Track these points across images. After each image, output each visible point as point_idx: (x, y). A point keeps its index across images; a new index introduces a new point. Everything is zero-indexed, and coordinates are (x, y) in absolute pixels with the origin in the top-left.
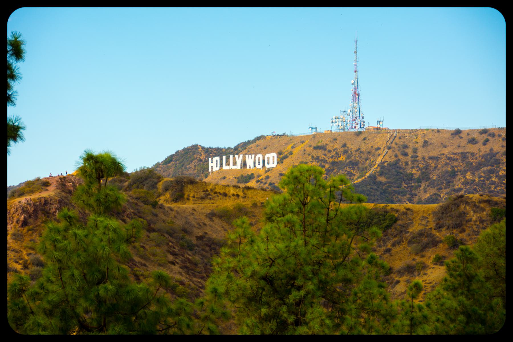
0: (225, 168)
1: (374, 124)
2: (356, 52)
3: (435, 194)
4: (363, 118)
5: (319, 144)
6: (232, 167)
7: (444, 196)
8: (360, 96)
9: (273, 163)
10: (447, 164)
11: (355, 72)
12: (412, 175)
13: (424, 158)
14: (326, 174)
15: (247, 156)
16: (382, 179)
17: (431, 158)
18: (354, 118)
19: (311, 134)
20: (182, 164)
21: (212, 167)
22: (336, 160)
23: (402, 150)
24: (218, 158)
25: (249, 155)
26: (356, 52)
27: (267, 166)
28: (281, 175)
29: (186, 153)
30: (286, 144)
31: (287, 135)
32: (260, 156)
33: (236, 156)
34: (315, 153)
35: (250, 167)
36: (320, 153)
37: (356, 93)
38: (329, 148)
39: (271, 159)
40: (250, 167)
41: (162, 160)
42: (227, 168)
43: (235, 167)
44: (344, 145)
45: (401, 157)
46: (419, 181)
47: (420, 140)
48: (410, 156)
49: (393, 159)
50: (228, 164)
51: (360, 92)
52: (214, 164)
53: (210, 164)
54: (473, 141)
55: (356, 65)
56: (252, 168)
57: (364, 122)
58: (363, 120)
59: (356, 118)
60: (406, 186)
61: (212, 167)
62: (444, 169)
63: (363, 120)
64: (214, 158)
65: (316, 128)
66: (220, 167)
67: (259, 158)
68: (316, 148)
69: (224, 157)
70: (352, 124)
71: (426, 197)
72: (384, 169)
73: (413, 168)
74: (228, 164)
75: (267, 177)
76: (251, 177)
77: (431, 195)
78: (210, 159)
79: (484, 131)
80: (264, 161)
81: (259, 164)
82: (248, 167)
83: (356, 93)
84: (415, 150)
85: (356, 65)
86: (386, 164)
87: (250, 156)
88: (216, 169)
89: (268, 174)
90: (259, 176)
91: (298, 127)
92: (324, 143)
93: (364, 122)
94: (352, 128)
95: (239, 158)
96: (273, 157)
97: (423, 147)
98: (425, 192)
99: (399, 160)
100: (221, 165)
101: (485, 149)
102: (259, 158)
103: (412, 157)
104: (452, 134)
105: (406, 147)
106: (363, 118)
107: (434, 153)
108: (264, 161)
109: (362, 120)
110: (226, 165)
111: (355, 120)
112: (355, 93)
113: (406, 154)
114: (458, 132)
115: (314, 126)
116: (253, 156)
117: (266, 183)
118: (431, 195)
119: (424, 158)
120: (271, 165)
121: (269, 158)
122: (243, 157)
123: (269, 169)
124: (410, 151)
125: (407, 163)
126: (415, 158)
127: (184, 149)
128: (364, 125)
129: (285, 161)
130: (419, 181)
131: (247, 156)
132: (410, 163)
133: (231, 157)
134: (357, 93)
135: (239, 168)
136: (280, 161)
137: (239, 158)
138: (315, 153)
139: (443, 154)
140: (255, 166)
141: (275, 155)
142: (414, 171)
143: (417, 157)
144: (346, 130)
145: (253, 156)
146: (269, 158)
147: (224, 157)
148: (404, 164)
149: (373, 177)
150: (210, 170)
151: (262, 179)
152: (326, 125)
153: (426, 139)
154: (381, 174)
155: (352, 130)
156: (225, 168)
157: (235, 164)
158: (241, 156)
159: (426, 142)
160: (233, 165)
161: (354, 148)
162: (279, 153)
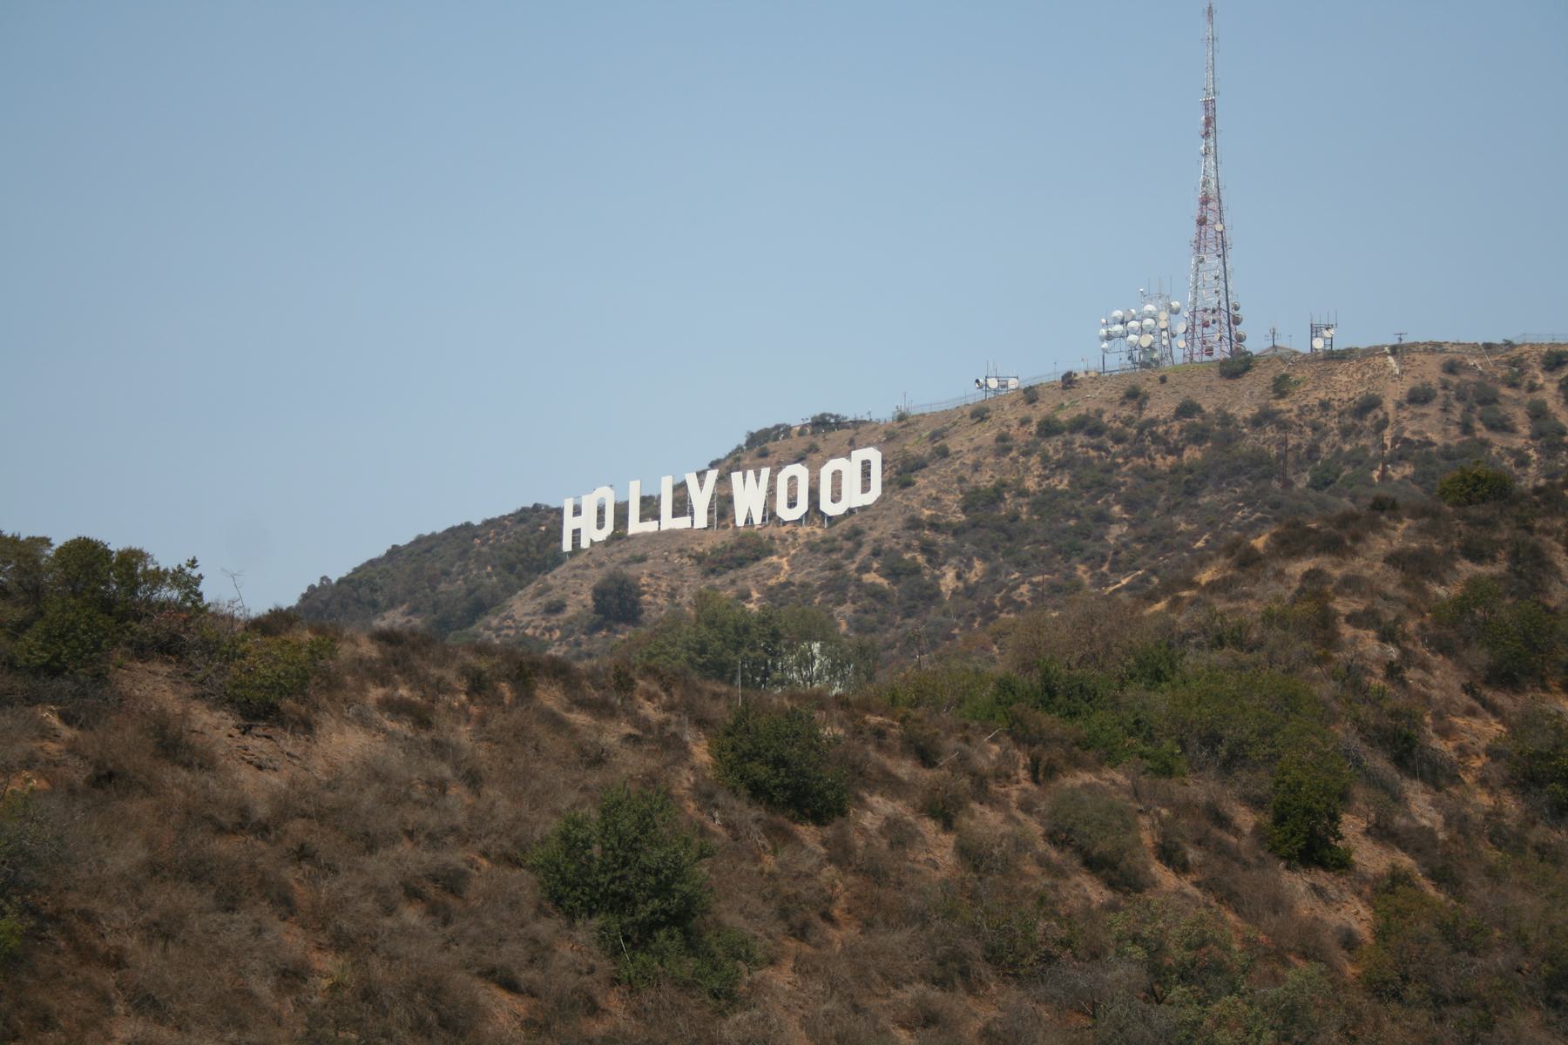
4: (1237, 321)
6: (668, 522)
9: (866, 488)
15: (736, 477)
21: (577, 532)
32: (800, 471)
35: (749, 520)
40: (749, 520)
42: (651, 526)
43: (683, 523)
55: (1209, 106)
56: (757, 520)
61: (577, 532)
71: (938, 994)
80: (814, 494)
81: (792, 504)
82: (740, 522)
85: (1209, 106)
95: (701, 483)
96: (866, 467)
108: (814, 494)
110: (642, 519)
116: (765, 472)
120: (854, 497)
121: (837, 476)
127: (420, 540)
131: (736, 477)
135: (701, 520)
137: (701, 483)
140: (773, 515)
150: (567, 546)
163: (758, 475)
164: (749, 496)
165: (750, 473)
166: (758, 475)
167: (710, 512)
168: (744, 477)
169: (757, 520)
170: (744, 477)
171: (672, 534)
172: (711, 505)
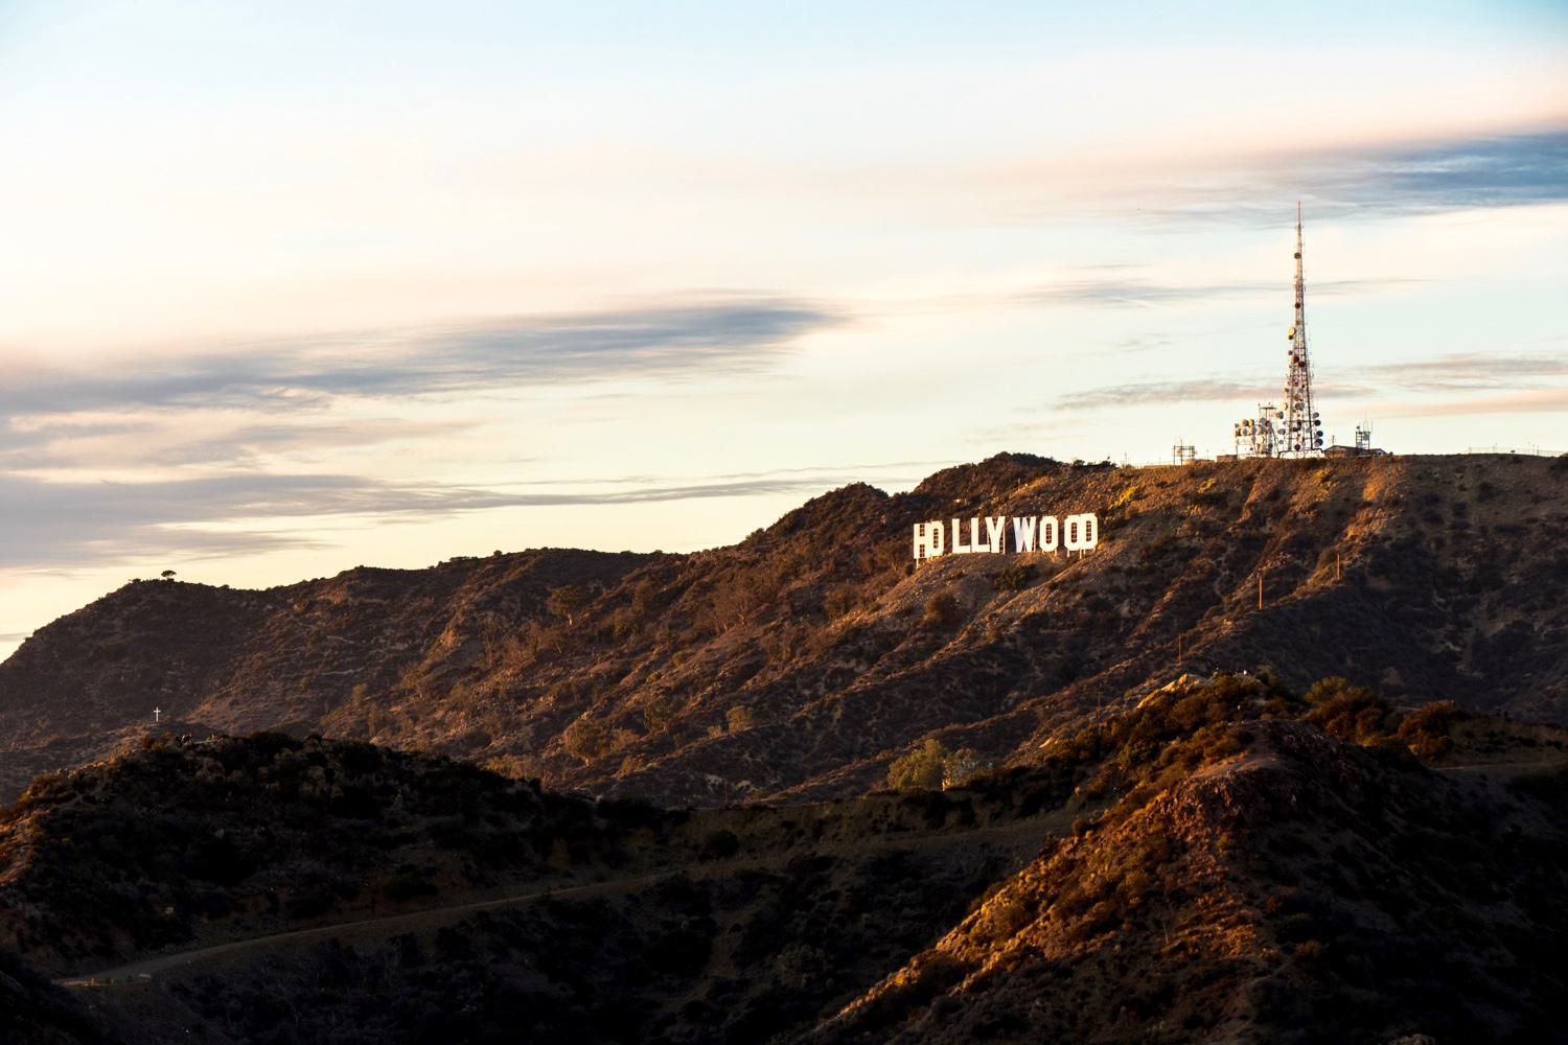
0: (958, 549)
2: (1298, 256)
3: (1517, 623)
4: (1318, 423)
6: (976, 547)
7: (1542, 629)
8: (1311, 369)
10: (1544, 546)
11: (1298, 306)
12: (1454, 571)
13: (1484, 530)
14: (1231, 569)
15: (1016, 521)
16: (1380, 584)
17: (1501, 530)
18: (1295, 425)
19: (1178, 463)
20: (828, 535)
21: (922, 546)
22: (1253, 531)
23: (1426, 508)
24: (939, 525)
25: (1021, 516)
26: (1298, 256)
27: (1070, 546)
29: (837, 506)
30: (1118, 488)
31: (1114, 465)
32: (1050, 520)
33: (989, 520)
37: (1300, 363)
39: (1082, 532)
41: (770, 524)
42: (965, 550)
43: (985, 549)
44: (1274, 495)
45: (1423, 527)
46: (1475, 587)
47: (1470, 481)
48: (1448, 524)
49: (1405, 533)
50: (966, 540)
51: (1311, 358)
52: (928, 540)
53: (917, 540)
56: (1029, 549)
57: (1320, 434)
58: (1319, 428)
59: (1299, 423)
60: (1442, 600)
61: (922, 546)
62: (1537, 558)
63: (1319, 428)
64: (927, 525)
65: (1192, 448)
66: (945, 545)
67: (1049, 527)
69: (956, 523)
70: (1290, 439)
73: (1456, 554)
74: (966, 540)
77: (1508, 626)
78: (917, 527)
80: (1061, 533)
82: (1019, 550)
84: (1460, 510)
86: (1387, 544)
87: (1024, 519)
88: (934, 552)
90: (1053, 571)
93: (1320, 434)
94: (1290, 449)
95: (995, 525)
96: (1089, 524)
97: (1481, 499)
98: (1493, 617)
99: (1420, 533)
102: (1049, 527)
103: (1453, 527)
104: (1552, 468)
105: (1434, 500)
106: (1318, 423)
107: (1509, 516)
108: (1061, 533)
109: (1315, 429)
111: (1296, 430)
112: (1296, 359)
113: (1436, 520)
115: (1186, 444)
116: (1033, 519)
117: (1075, 592)
118: (1508, 626)
119: (1484, 530)
122: (1006, 520)
123: (1076, 553)
124: (1449, 517)
125: (1440, 543)
126: (1460, 528)
128: (1321, 442)
130: (1475, 587)
131: (1016, 521)
132: (1448, 542)
133: (975, 522)
134: (1302, 359)
135: (996, 549)
136: (1107, 531)
137: (995, 525)
139: (1534, 520)
140: (1038, 547)
141: (1092, 518)
142: (1461, 563)
143: (1468, 526)
144: (1274, 456)
145: (1033, 519)
146: (1074, 527)
147: (956, 523)
148: (1433, 545)
150: (917, 555)
151: (1064, 581)
153: (1487, 479)
154: (1378, 569)
155: (1290, 456)
157: (984, 539)
158: (1001, 520)
159: (1485, 487)
160: (980, 543)
162: (1102, 514)
163: (1028, 520)
164: (1025, 533)
165: (1024, 519)
166: (1028, 520)
167: (1001, 543)
168: (1021, 520)
169: (1029, 549)
170: (1021, 520)
171: (977, 554)
172: (1001, 539)
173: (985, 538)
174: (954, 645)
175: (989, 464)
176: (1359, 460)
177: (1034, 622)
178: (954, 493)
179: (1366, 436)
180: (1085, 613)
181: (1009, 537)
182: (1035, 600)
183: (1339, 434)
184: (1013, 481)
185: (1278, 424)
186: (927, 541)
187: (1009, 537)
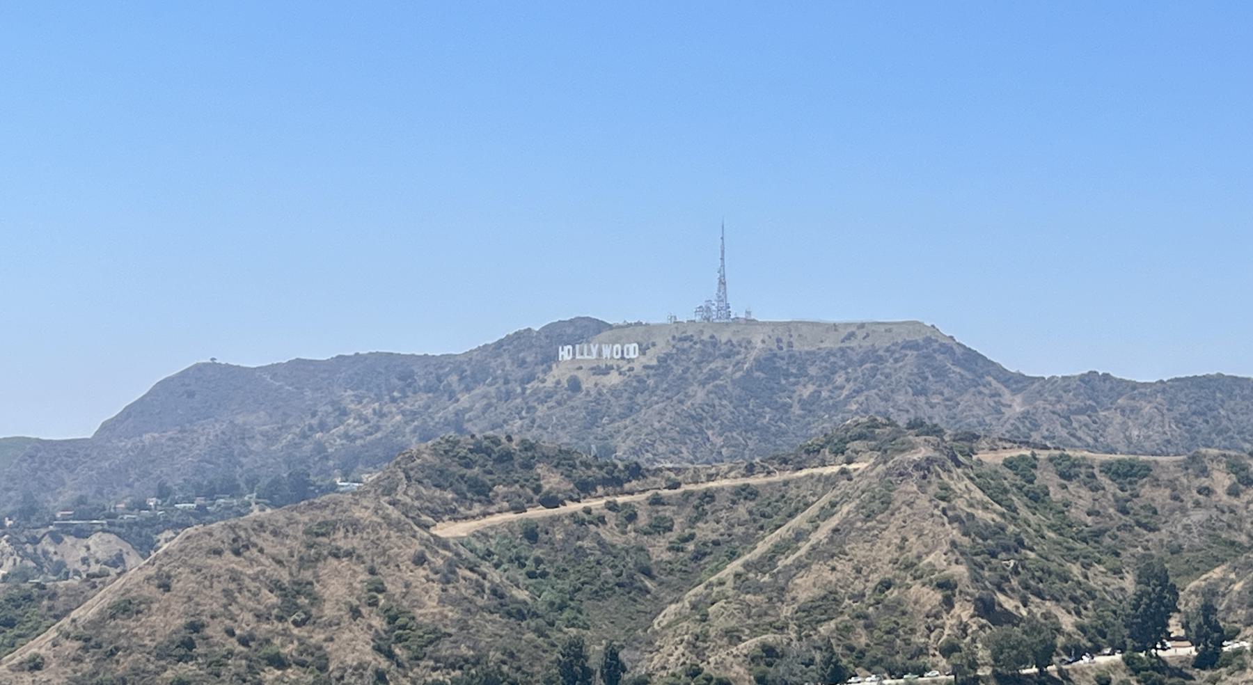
1: (742, 315)
5: (683, 337)
6: (586, 357)
17: (808, 353)
24: (570, 347)
28: (646, 367)
32: (618, 346)
34: (679, 345)
36: (687, 345)
37: (722, 283)
38: (695, 338)
39: (632, 350)
53: (561, 353)
54: (851, 336)
55: (723, 252)
68: (680, 340)
72: (759, 364)
75: (631, 369)
76: (612, 368)
79: (862, 326)
83: (722, 283)
84: (790, 345)
89: (631, 365)
91: (657, 317)
92: (689, 334)
100: (574, 354)
101: (867, 344)
113: (781, 348)
114: (835, 327)
120: (632, 356)
129: (650, 352)
136: (643, 351)
138: (679, 345)
147: (577, 346)
149: (749, 371)
152: (686, 314)
156: (578, 357)
157: (590, 353)
161: (724, 340)
162: (640, 345)
164: (606, 352)
173: (590, 353)
174: (579, 399)
175: (571, 321)
176: (750, 322)
177: (614, 391)
178: (559, 334)
179: (748, 313)
180: (635, 384)
181: (600, 353)
182: (614, 379)
183: (737, 312)
184: (585, 330)
185: (714, 308)
186: (565, 353)
187: (600, 353)
